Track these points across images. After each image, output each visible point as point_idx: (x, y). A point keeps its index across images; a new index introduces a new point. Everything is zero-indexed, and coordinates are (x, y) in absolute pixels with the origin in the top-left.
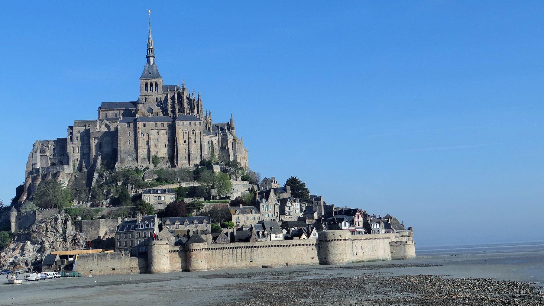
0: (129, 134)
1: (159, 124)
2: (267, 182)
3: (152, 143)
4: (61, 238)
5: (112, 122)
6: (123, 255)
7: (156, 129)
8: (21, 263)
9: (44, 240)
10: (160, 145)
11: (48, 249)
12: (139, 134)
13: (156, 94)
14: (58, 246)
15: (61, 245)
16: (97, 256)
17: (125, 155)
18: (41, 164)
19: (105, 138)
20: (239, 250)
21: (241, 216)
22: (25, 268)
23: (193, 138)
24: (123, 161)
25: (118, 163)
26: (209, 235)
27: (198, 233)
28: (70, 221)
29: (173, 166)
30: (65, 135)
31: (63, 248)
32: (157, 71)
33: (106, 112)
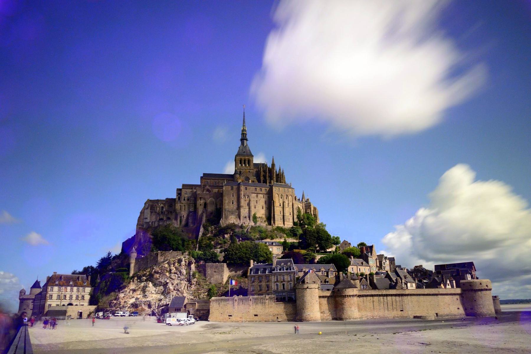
0: (233, 195)
1: (258, 189)
2: (346, 244)
3: (252, 205)
4: (185, 281)
5: (213, 188)
6: (267, 299)
7: (256, 192)
8: (143, 305)
9: (168, 281)
10: (259, 207)
11: (172, 292)
12: (242, 196)
13: (249, 169)
14: (182, 289)
15: (186, 288)
16: (237, 299)
17: (228, 213)
18: (151, 219)
19: (210, 199)
20: (389, 298)
21: (355, 267)
22: (148, 311)
23: (287, 202)
24: (226, 218)
25: (223, 219)
26: (357, 281)
27: (348, 277)
28: (194, 264)
29: (270, 224)
30: (174, 196)
31: (188, 290)
32: (250, 151)
33: (207, 180)
